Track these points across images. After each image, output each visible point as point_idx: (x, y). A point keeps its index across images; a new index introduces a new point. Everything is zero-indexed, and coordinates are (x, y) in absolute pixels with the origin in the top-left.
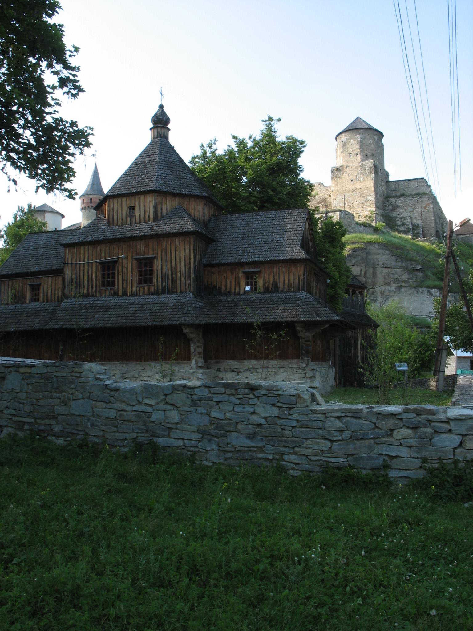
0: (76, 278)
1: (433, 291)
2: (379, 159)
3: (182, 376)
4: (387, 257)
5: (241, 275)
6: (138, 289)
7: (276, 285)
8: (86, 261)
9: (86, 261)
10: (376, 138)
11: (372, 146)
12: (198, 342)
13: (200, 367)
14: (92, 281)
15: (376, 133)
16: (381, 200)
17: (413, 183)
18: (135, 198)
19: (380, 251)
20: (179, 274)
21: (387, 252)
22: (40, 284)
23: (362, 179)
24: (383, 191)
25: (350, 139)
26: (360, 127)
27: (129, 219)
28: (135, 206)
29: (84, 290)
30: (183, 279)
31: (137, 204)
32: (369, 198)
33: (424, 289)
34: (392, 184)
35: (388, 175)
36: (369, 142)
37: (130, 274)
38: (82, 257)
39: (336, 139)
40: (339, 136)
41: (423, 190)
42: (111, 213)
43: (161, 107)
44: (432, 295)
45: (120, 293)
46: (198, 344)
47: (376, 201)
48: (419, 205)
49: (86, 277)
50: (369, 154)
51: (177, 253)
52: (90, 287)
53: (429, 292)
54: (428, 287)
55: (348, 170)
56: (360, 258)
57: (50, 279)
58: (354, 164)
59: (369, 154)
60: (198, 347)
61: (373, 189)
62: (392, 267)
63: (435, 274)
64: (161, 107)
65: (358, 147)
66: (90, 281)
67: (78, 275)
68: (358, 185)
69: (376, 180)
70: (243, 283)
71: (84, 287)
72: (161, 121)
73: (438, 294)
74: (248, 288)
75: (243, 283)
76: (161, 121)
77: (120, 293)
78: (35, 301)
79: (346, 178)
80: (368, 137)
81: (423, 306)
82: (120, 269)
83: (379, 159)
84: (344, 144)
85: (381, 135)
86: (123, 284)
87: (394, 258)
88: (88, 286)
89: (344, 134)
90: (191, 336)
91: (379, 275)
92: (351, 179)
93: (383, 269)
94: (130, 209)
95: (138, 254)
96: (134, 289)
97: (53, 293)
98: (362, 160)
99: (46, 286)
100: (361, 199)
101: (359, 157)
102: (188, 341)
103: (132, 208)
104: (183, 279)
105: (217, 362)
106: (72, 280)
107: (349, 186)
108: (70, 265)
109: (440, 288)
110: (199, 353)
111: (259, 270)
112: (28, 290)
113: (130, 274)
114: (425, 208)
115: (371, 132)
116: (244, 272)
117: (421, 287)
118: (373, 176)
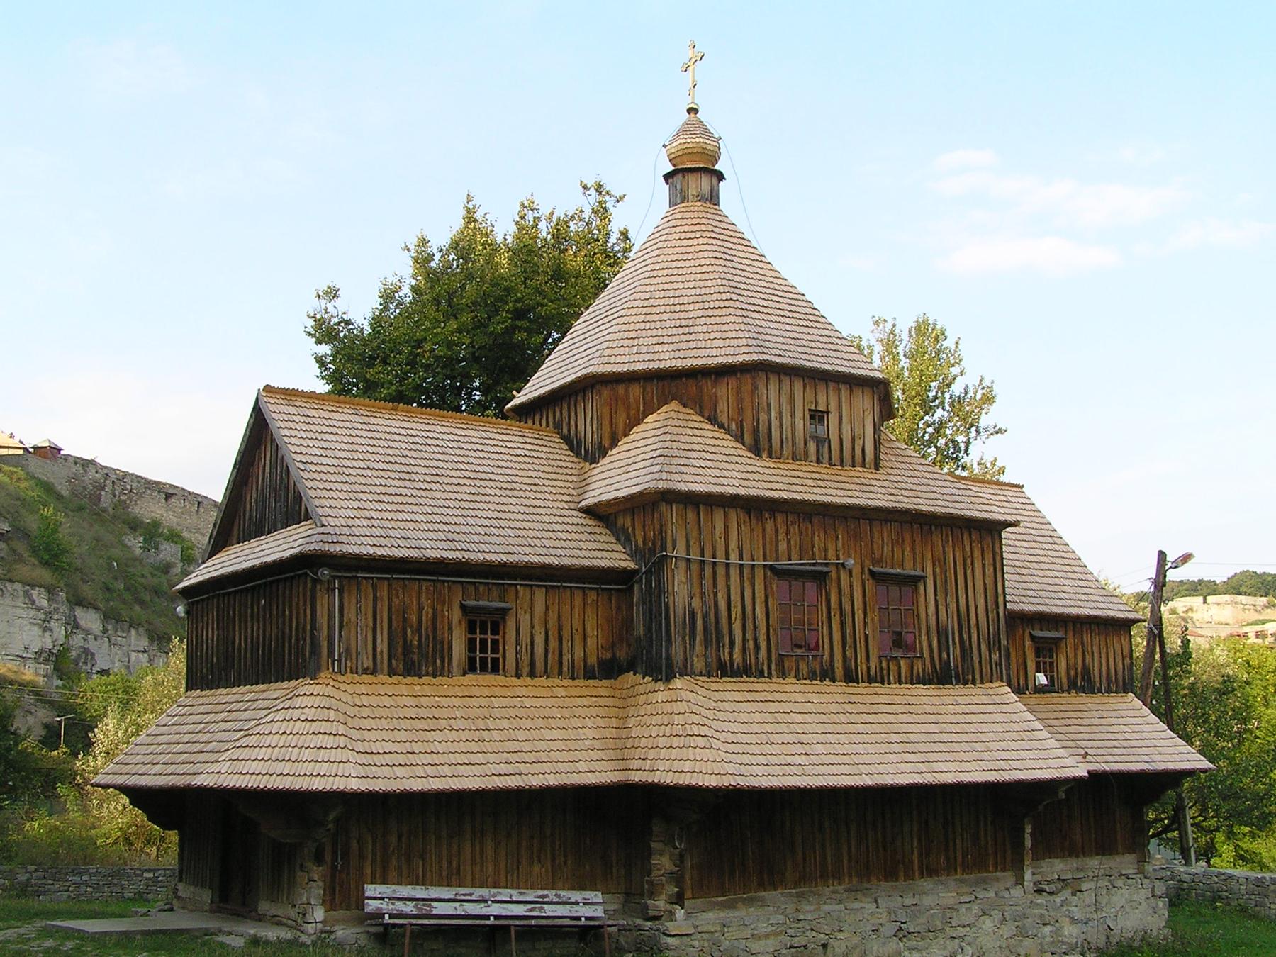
0: (705, 617)
1: (35, 593)
3: (1042, 916)
5: (1028, 643)
6: (884, 665)
7: (1086, 672)
8: (734, 559)
9: (734, 559)
14: (755, 627)
18: (791, 382)
20: (974, 631)
22: (504, 612)
27: (812, 447)
28: (828, 413)
29: (731, 654)
30: (983, 647)
31: (833, 407)
33: (18, 586)
37: (859, 615)
38: (720, 544)
42: (763, 417)
44: (33, 602)
45: (839, 671)
49: (736, 613)
51: (969, 572)
52: (751, 644)
53: (27, 594)
54: (25, 583)
57: (540, 595)
63: (34, 552)
66: (750, 626)
67: (709, 600)
70: (1031, 664)
71: (732, 643)
73: (45, 603)
74: (1042, 679)
75: (1031, 664)
77: (839, 671)
78: (484, 669)
81: (12, 630)
88: (744, 641)
94: (812, 417)
95: (879, 562)
97: (553, 644)
99: (525, 620)
103: (817, 416)
104: (983, 647)
106: (693, 615)
108: (682, 565)
109: (51, 590)
112: (455, 622)
113: (859, 615)
116: (1033, 638)
117: (11, 581)
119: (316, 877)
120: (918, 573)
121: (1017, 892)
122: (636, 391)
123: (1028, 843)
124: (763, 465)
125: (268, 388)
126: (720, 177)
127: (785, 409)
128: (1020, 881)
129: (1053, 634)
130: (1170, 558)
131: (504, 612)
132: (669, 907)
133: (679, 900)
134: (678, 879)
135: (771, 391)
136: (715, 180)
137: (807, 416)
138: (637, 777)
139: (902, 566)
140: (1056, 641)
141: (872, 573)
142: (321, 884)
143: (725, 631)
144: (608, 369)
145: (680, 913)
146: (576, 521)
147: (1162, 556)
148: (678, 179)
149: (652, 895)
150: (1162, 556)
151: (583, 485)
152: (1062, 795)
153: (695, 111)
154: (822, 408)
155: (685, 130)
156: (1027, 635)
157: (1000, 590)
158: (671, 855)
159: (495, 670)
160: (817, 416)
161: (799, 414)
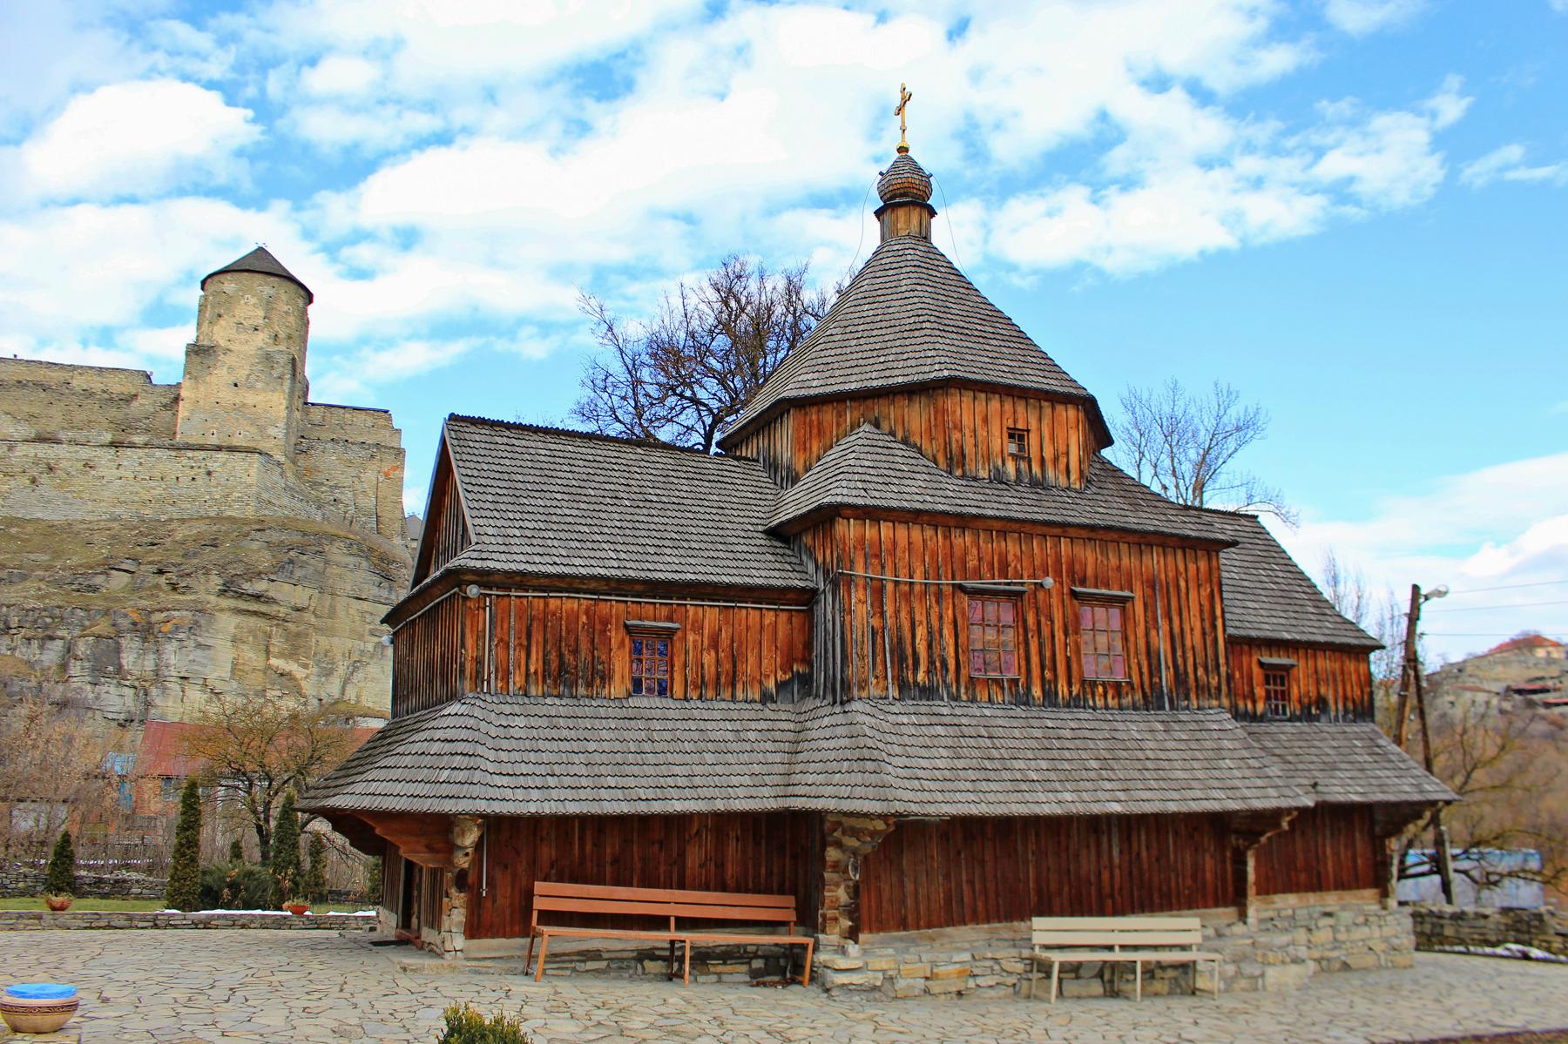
5: (1256, 669)
10: (301, 303)
11: (292, 319)
17: (362, 416)
19: (351, 559)
21: (365, 564)
23: (259, 385)
31: (1033, 425)
32: (272, 431)
36: (286, 308)
37: (1059, 635)
39: (204, 283)
40: (216, 278)
41: (383, 437)
42: (956, 436)
43: (902, 150)
48: (373, 466)
49: (921, 632)
55: (230, 360)
56: (311, 569)
58: (246, 347)
59: (282, 335)
61: (284, 414)
64: (902, 150)
65: (261, 313)
68: (250, 398)
77: (1037, 691)
79: (220, 376)
80: (284, 297)
85: (309, 297)
86: (1042, 668)
89: (229, 276)
91: (341, 613)
92: (233, 380)
94: (1011, 436)
95: (1083, 583)
96: (1075, 690)
100: (253, 430)
107: (228, 396)
114: (387, 475)
115: (293, 287)
116: (1261, 664)
118: (287, 384)
119: (457, 903)
120: (1126, 593)
121: (1239, 929)
122: (829, 415)
123: (1251, 876)
124: (952, 485)
125: (454, 418)
126: (932, 213)
127: (981, 426)
128: (1243, 916)
129: (1284, 661)
130: (1423, 591)
131: (671, 633)
132: (842, 942)
133: (853, 934)
134: (853, 912)
135: (963, 409)
136: (925, 215)
137: (1005, 435)
138: (798, 804)
139: (1107, 586)
140: (1287, 669)
141: (1074, 594)
142: (463, 911)
143: (909, 651)
144: (803, 392)
145: (853, 949)
146: (758, 542)
147: (1416, 588)
148: (887, 216)
149: (823, 931)
150: (1416, 588)
151: (776, 510)
152: (1285, 825)
153: (907, 150)
154: (1020, 426)
155: (895, 166)
156: (1254, 660)
157: (1218, 613)
158: (847, 887)
159: (662, 692)
160: (1017, 435)
161: (997, 433)
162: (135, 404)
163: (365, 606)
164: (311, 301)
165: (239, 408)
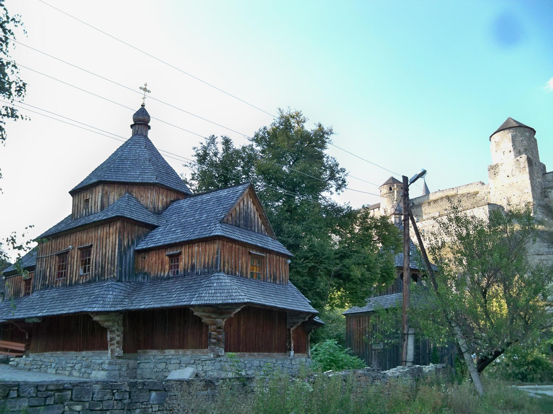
2: (533, 153)
4: (538, 244)
10: (527, 134)
11: (525, 142)
12: (118, 330)
13: (119, 357)
15: (527, 129)
16: (539, 191)
24: (540, 183)
25: (502, 139)
26: (511, 126)
32: (526, 191)
34: (549, 175)
35: (544, 167)
36: (521, 139)
39: (490, 140)
43: (143, 106)
46: (117, 333)
47: (533, 193)
50: (522, 150)
59: (522, 150)
60: (117, 336)
62: (545, 253)
64: (143, 106)
69: (531, 173)
72: (141, 121)
76: (141, 121)
79: (502, 174)
80: (519, 135)
82: (70, 260)
83: (533, 153)
84: (497, 143)
87: (546, 244)
90: (106, 324)
93: (535, 256)
98: (516, 156)
100: (519, 192)
101: (513, 153)
102: (104, 331)
105: (145, 352)
110: (118, 343)
111: (179, 251)
115: (522, 129)
162: (478, 195)
163: (543, 257)
164: (535, 132)
165: (511, 185)
